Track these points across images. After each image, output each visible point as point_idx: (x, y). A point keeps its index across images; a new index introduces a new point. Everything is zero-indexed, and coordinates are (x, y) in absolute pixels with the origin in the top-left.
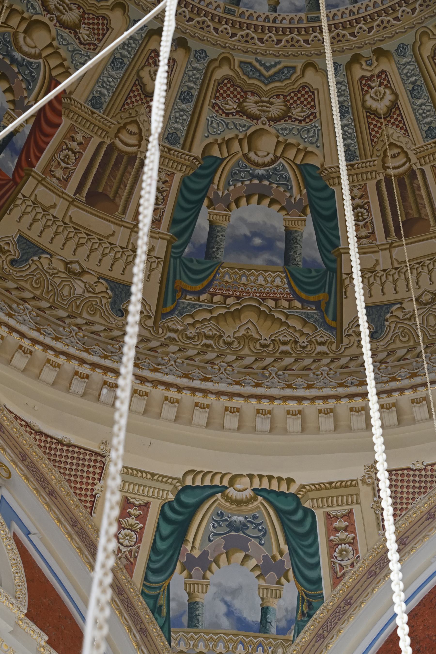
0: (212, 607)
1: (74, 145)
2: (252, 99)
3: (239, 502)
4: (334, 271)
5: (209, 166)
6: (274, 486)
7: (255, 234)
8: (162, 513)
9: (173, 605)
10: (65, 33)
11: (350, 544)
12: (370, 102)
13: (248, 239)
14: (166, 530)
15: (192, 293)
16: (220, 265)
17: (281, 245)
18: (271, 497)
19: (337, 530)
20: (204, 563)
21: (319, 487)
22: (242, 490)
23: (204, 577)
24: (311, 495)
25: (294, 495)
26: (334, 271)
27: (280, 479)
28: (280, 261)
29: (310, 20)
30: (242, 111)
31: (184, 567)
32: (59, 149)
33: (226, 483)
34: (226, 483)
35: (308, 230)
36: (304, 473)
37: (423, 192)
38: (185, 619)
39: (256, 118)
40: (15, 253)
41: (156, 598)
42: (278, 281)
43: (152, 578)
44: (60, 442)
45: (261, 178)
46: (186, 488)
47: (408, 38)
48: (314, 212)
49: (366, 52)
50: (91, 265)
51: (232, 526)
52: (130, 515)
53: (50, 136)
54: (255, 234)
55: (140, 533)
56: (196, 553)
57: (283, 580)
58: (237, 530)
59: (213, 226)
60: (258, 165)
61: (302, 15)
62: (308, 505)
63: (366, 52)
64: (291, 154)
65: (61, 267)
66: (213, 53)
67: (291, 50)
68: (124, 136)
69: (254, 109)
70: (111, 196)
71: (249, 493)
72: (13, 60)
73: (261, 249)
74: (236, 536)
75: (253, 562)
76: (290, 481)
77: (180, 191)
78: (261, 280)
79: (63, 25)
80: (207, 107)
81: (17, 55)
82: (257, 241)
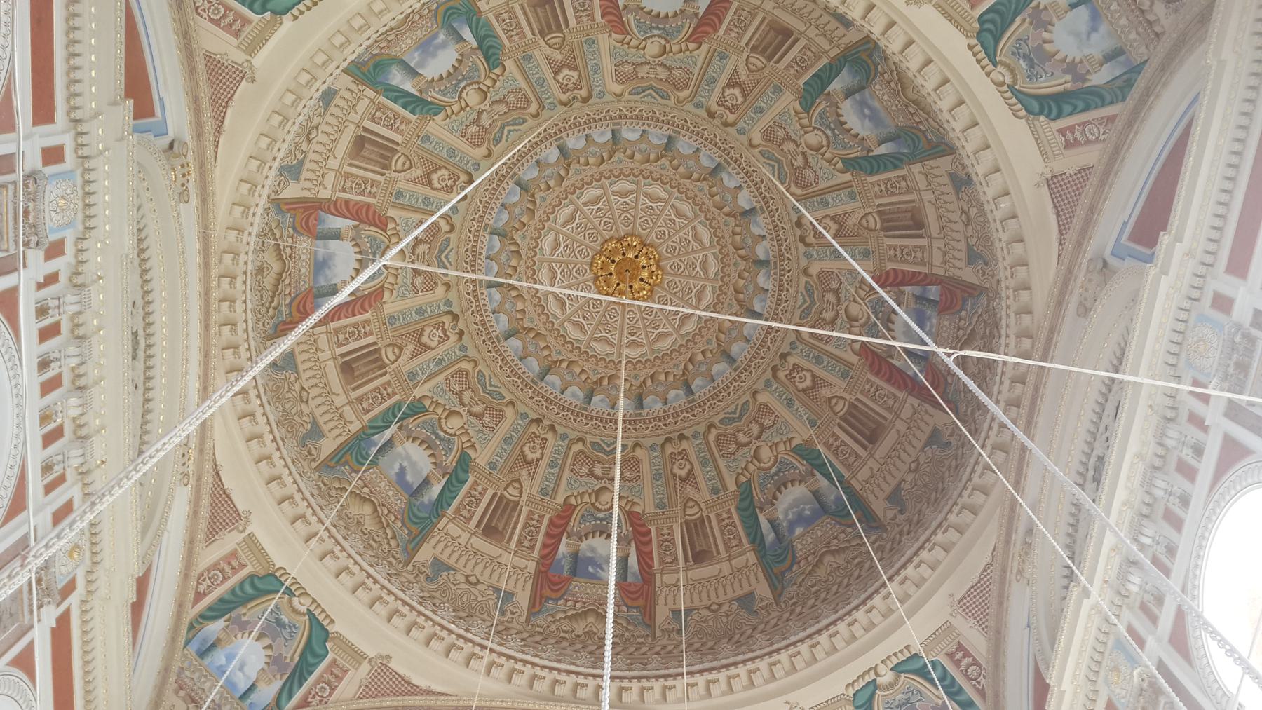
0: (1099, 44)
1: (898, 253)
3: (1012, 71)
4: (844, 56)
6: (982, 54)
7: (865, 116)
8: (1058, 116)
9: (1118, 73)
12: (740, 99)
13: (871, 118)
14: (1067, 108)
16: (897, 126)
17: (857, 96)
20: (1071, 68)
21: (959, 26)
22: (1001, 73)
23: (1081, 62)
24: (968, 28)
25: (978, 37)
26: (844, 56)
27: (975, 55)
28: (867, 92)
30: (807, 164)
31: (1085, 80)
32: (905, 262)
33: (1005, 88)
34: (1005, 88)
35: (836, 86)
37: (757, 36)
38: (1122, 58)
39: (803, 154)
40: (980, 265)
41: (1120, 88)
42: (878, 87)
43: (1108, 98)
44: (1058, 215)
45: (832, 130)
46: (1029, 112)
47: (689, 107)
48: (823, 88)
51: (1031, 65)
52: (1075, 139)
53: (903, 271)
54: (865, 116)
55: (1083, 124)
56: (1069, 77)
57: (1042, 7)
58: (1032, 60)
60: (827, 136)
62: (977, 25)
63: (717, 122)
64: (805, 122)
69: (800, 158)
73: (869, 107)
74: (1037, 58)
75: (1045, 35)
76: (970, 47)
77: (877, 172)
78: (886, 97)
79: (839, 300)
80: (821, 187)
82: (867, 112)
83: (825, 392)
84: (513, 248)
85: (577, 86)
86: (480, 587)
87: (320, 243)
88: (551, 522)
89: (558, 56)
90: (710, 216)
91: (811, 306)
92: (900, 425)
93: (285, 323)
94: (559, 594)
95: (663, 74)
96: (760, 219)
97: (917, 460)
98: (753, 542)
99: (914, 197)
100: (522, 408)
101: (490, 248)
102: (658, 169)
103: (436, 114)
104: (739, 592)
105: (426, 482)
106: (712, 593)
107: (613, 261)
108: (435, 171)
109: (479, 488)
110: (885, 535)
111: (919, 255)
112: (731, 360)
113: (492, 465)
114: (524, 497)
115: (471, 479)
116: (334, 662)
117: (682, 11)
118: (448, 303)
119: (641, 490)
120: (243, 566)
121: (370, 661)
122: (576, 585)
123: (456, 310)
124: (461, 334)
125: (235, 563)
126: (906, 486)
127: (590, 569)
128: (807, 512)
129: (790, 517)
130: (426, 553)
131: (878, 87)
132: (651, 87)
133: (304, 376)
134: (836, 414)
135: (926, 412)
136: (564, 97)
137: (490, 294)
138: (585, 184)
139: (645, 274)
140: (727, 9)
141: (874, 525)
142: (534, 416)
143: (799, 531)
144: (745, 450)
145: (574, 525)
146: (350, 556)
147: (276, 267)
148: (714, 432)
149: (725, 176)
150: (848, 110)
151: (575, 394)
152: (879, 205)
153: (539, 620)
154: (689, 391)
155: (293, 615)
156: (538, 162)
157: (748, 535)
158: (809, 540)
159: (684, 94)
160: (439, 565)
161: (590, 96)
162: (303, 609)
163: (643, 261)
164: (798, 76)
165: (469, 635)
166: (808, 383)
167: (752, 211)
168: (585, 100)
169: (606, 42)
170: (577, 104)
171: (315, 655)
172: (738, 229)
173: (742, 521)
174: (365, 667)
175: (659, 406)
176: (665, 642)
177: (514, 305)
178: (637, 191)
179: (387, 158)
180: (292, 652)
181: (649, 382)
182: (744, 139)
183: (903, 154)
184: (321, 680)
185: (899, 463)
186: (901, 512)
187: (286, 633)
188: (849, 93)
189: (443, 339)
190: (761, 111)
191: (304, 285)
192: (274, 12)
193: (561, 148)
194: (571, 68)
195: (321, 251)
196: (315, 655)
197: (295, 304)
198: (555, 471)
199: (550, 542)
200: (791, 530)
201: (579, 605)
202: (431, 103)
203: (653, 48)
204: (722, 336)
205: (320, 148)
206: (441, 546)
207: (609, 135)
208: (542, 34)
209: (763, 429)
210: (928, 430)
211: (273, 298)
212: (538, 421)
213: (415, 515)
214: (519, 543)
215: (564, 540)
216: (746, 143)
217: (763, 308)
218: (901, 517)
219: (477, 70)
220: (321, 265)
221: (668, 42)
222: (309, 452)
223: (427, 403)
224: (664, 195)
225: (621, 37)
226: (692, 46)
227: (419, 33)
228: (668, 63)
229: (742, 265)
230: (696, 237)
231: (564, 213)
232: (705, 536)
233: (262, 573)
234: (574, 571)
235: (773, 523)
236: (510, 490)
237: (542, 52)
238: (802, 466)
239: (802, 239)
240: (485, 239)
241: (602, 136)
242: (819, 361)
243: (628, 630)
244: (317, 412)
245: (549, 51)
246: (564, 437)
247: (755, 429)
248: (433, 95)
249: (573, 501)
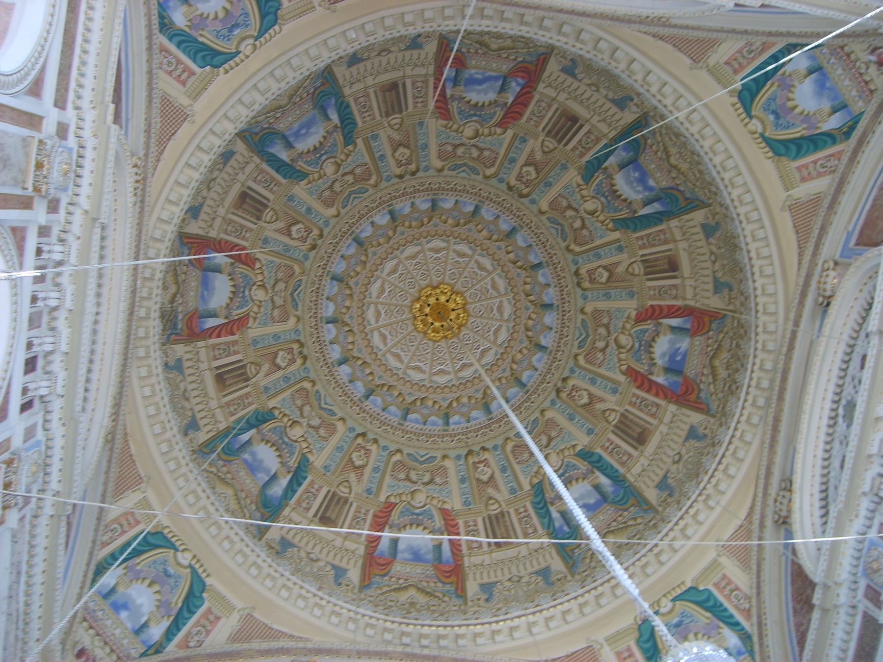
1: (420, 100)
2: (352, 181)
3: (243, 39)
4: (259, 152)
5: (349, 139)
6: (231, 63)
10: (458, 142)
11: (171, 71)
12: (300, 226)
15: (319, 87)
16: (314, 108)
17: (291, 140)
18: (228, 57)
19: (184, 71)
21: (210, 82)
22: (246, 47)
24: (210, 76)
27: (232, 68)
28: (287, 133)
29: (353, 232)
34: (257, 43)
35: (284, 155)
36: (223, 82)
37: (248, 217)
45: (322, 155)
46: (275, 23)
47: (308, 264)
49: (319, 242)
50: (376, 61)
51: (236, 26)
57: (188, 24)
58: (233, 26)
59: (328, 119)
61: (358, 231)
63: (319, 242)
65: (392, 49)
66: (384, 184)
67: (350, 214)
68: (398, 121)
69: (347, 178)
70: (387, 93)
71: (242, 48)
72: (475, 115)
76: (226, 72)
77: (354, 119)
79: (462, 145)
81: (475, 118)
82: (303, 131)
83: (538, 156)
84: (418, 403)
85: (290, 351)
86: (683, 452)
87: (399, 556)
88: (639, 387)
89: (266, 367)
90: (396, 246)
91: (468, 167)
92: (562, 97)
93: (457, 589)
94: (696, 387)
95: (281, 286)
96: (398, 207)
97: (589, 85)
98: (661, 221)
99: (371, 91)
100: (547, 404)
101: (417, 421)
102: (358, 287)
103: (308, 460)
104: (701, 236)
105: (597, 488)
106: (702, 258)
107: (432, 324)
108: (353, 462)
109: (607, 444)
110: (651, 114)
111: (419, 84)
112: (513, 231)
113: (590, 432)
114: (617, 408)
115: (599, 450)
116: (716, 585)
117: (229, 275)
118: (458, 457)
119: (619, 310)
120: (629, 649)
121: (719, 556)
122: (691, 370)
123: (464, 452)
124: (484, 449)
125: (626, 654)
126: (611, 95)
127: (678, 358)
128: (637, 174)
129: (640, 188)
130: (652, 495)
131: (282, 125)
132: (292, 294)
133: (500, 578)
134: (556, 148)
135: (549, 77)
136: (299, 361)
137: (455, 423)
138: (369, 345)
139: (443, 299)
140: (227, 242)
141: (643, 122)
142: (553, 395)
143: (651, 183)
144: (587, 222)
145: (642, 368)
146: (633, 564)
147: (412, 592)
148: (572, 247)
149: (364, 235)
150: (303, 145)
151: (539, 360)
152: (381, 116)
153: (714, 406)
154: (539, 265)
155: (674, 613)
156: (351, 381)
157: (656, 224)
158: (659, 175)
159: (297, 269)
160: (662, 485)
161: (298, 341)
162: (670, 605)
163: (432, 301)
164: (278, 184)
165: (710, 472)
166: (531, 169)
167: (391, 213)
168: (302, 345)
169: (254, 331)
170: (305, 351)
171: (708, 600)
172: (407, 224)
173: (645, 228)
174: (724, 560)
175: (551, 290)
176: (738, 303)
177: (464, 405)
178: (376, 304)
179: (339, 500)
180: (703, 617)
181: (532, 298)
182: (333, 221)
183: (336, 101)
184: (728, 597)
185: (593, 100)
186: (632, 100)
187: (687, 621)
188: (289, 146)
189: (485, 462)
190: (309, 210)
191: (430, 571)
192: (203, 591)
193: (341, 363)
194: (276, 357)
195: (407, 556)
196: (708, 600)
197: (444, 579)
198: (599, 380)
199: (654, 391)
200: (650, 189)
201: (705, 372)
202: (299, 463)
203: (260, 295)
204: (495, 237)
205: (325, 551)
206: (648, 481)
207: (330, 326)
208: (247, 380)
209: (570, 207)
210: (563, 76)
211: (436, 597)
212: (558, 391)
213: (622, 499)
214: (653, 416)
215: (654, 378)
216: (338, 219)
217: (471, 204)
218: (636, 100)
219: (275, 428)
220: (417, 557)
221: (254, 284)
222: (559, 580)
223: (536, 481)
224: (379, 282)
225: (251, 320)
226: (258, 265)
227: (242, 474)
228: (272, 282)
229: (435, 220)
230: (413, 257)
231: (393, 362)
232: (656, 260)
233: (636, 634)
234: (679, 372)
235: (647, 203)
236: (611, 418)
237: (262, 379)
238: (599, 177)
239: (413, 174)
240: (409, 425)
241: (330, 332)
242: (513, 161)
243: (726, 333)
244: (530, 570)
245: (262, 374)
246: (572, 371)
247: (570, 213)
248: (293, 462)
249: (624, 368)
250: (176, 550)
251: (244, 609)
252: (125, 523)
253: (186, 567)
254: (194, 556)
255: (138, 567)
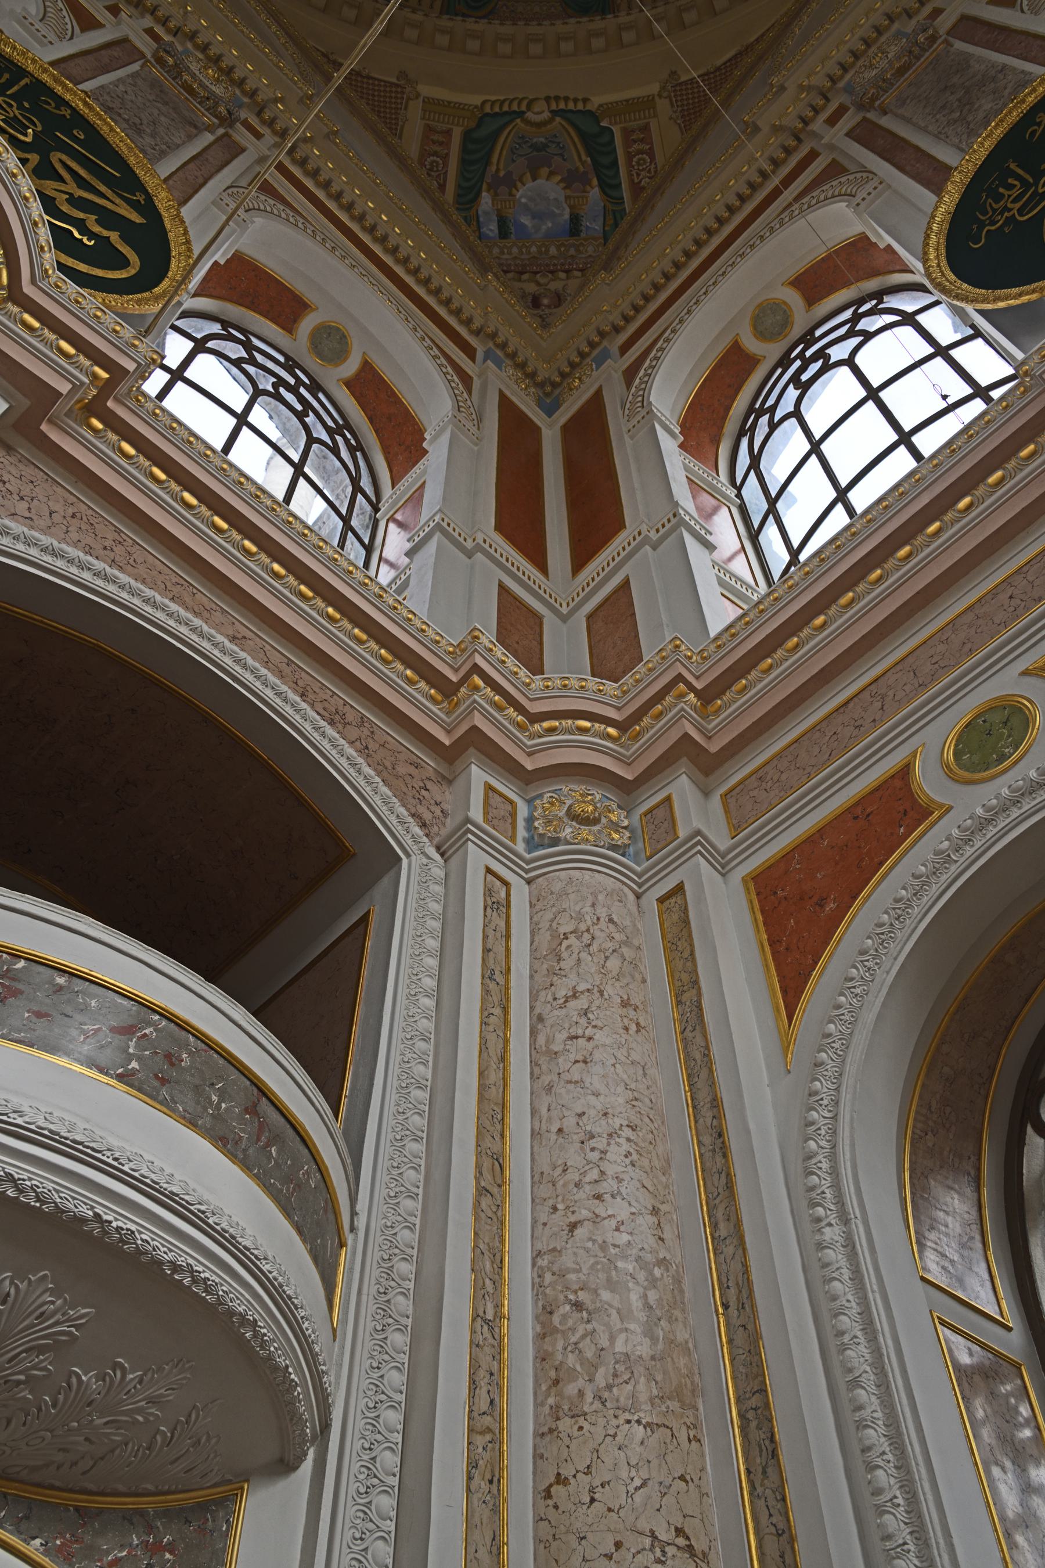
250: (521, 114)
251: (663, 88)
252: (436, 148)
253: (551, 120)
254: (547, 99)
255: (502, 174)
